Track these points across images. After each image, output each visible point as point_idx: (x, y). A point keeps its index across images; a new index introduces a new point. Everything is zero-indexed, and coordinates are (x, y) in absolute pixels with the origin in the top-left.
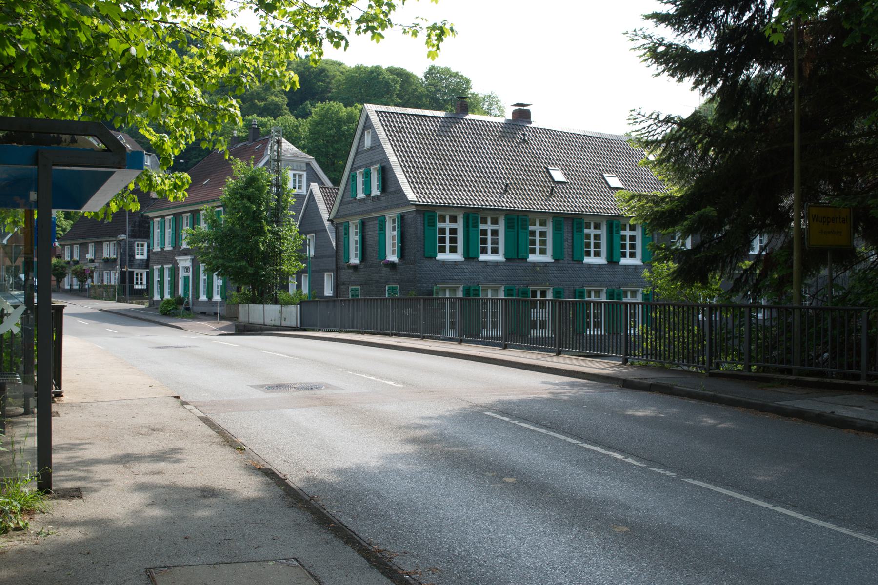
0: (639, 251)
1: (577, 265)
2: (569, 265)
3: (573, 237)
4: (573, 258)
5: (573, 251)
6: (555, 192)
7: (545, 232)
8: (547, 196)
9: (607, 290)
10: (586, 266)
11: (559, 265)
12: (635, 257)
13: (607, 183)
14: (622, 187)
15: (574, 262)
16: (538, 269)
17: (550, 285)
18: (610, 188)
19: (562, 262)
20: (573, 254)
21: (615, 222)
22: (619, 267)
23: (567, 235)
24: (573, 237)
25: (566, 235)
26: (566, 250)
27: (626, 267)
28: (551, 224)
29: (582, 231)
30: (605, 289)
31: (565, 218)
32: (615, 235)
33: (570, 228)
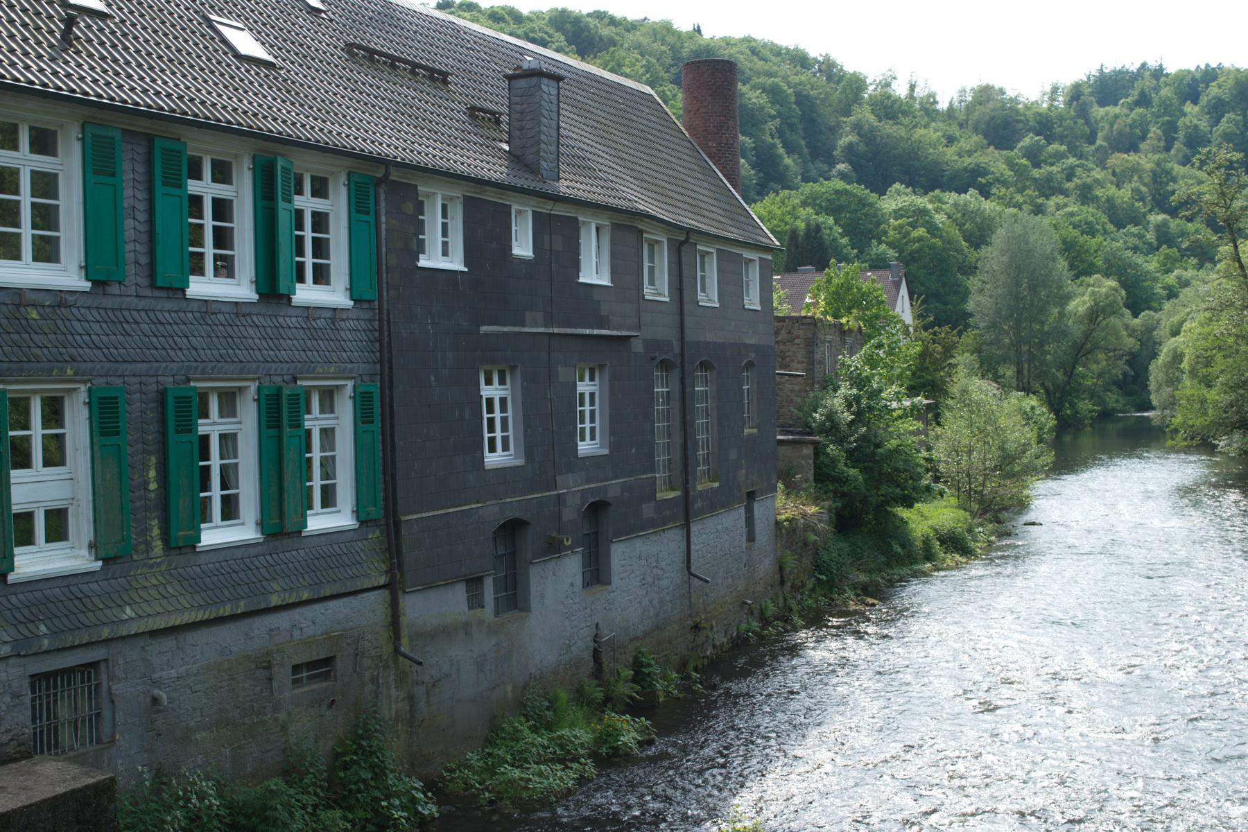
0: (339, 261)
1: (168, 305)
2: (142, 304)
3: (151, 202)
4: (152, 276)
5: (152, 253)
6: (78, 38)
7: (54, 177)
8: (51, 46)
9: (259, 390)
10: (195, 306)
11: (108, 302)
12: (328, 283)
13: (224, 41)
14: (270, 58)
15: (157, 293)
16: (34, 315)
17: (79, 377)
18: (238, 56)
19: (115, 289)
20: (152, 265)
21: (280, 163)
22: (291, 312)
23: (131, 194)
24: (151, 202)
25: (128, 192)
26: (131, 247)
27: (309, 311)
28: (77, 148)
29: (180, 185)
30: (253, 387)
31: (125, 131)
32: (281, 204)
33: (141, 169)
